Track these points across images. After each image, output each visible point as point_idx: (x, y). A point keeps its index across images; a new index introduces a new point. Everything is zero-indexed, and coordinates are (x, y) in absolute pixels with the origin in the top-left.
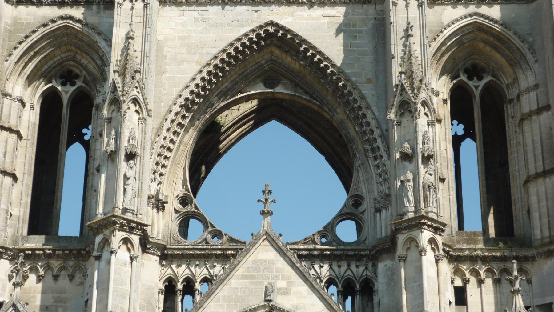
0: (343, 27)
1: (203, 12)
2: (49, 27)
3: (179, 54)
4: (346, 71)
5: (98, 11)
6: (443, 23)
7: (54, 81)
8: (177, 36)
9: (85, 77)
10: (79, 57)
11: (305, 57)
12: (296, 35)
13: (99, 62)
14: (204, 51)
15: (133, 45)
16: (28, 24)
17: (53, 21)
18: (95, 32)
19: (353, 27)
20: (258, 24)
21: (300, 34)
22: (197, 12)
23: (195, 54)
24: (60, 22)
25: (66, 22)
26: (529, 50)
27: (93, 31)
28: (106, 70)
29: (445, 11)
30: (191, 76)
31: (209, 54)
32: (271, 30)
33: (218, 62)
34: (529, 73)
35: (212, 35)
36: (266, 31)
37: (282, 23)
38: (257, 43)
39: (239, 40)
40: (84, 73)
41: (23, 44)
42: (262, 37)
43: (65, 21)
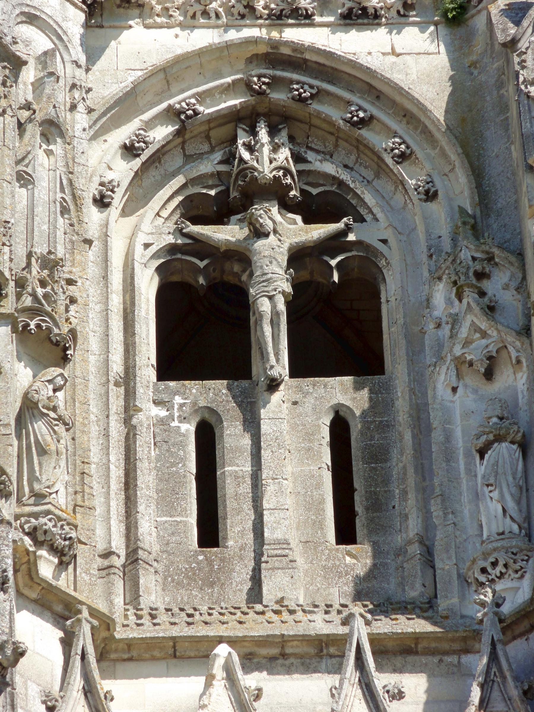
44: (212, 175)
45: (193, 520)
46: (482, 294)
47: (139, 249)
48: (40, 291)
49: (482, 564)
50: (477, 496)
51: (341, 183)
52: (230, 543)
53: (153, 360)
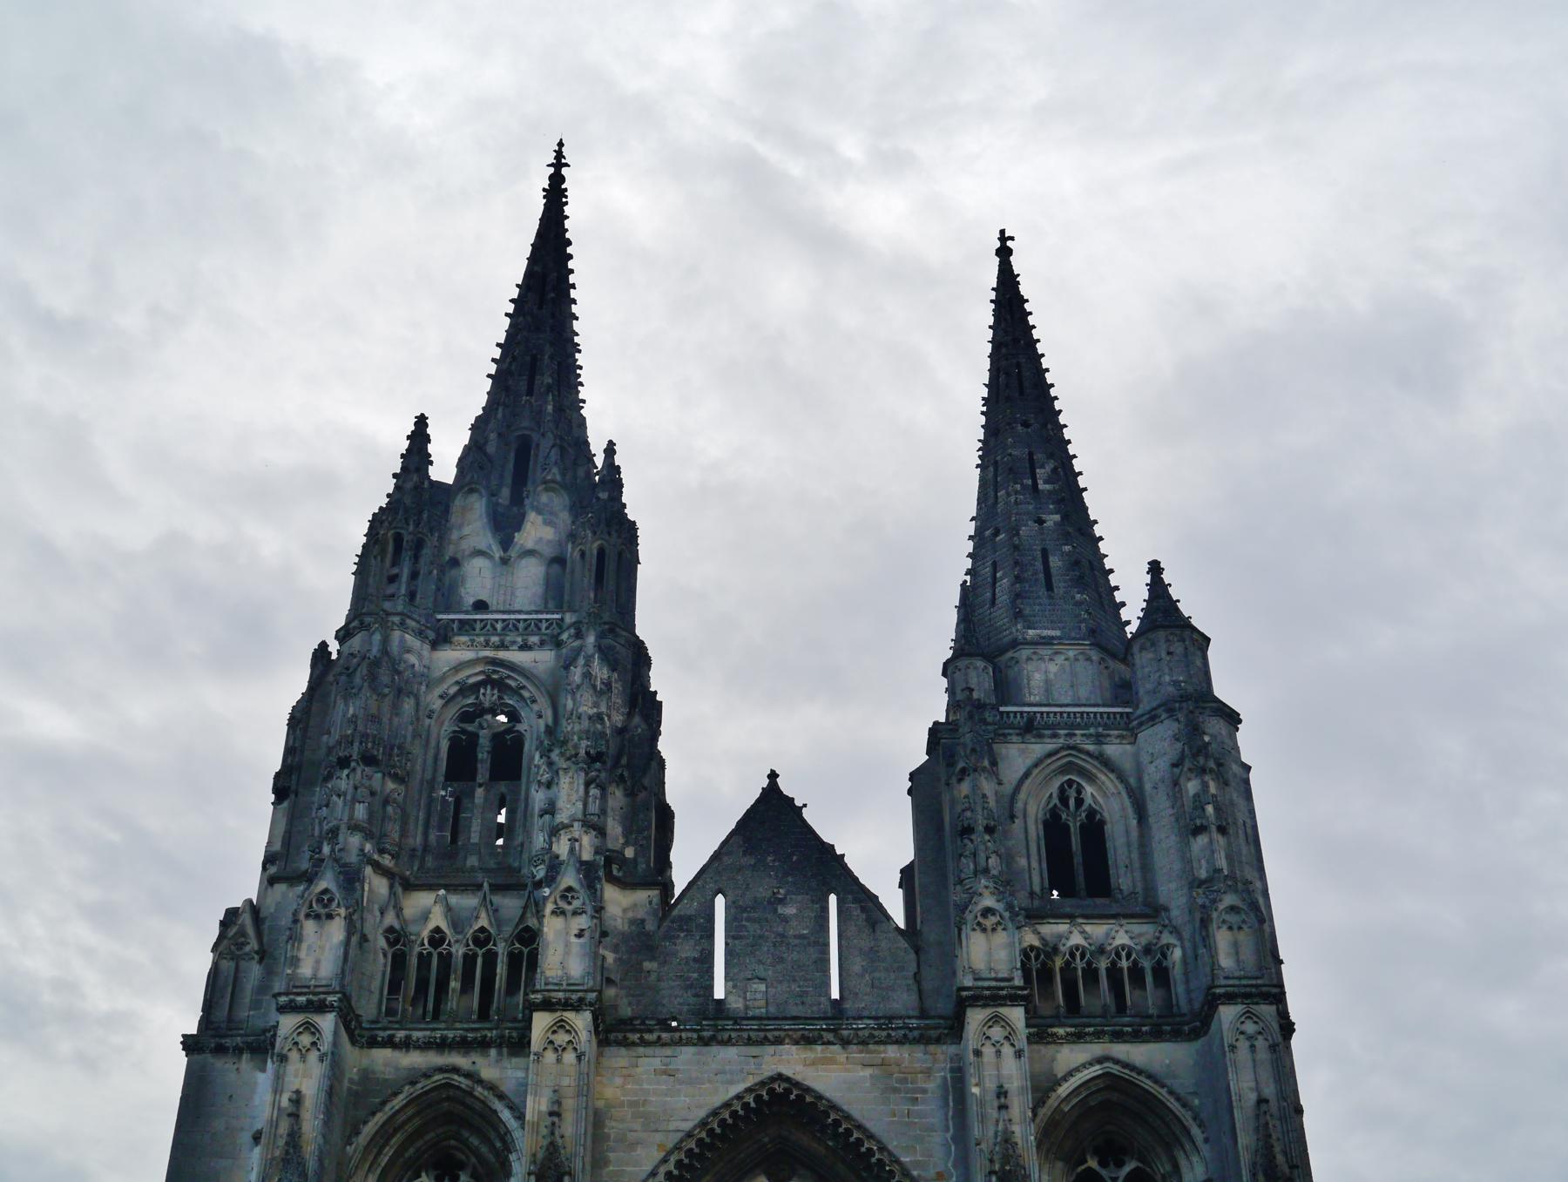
0: (896, 1083)
1: (669, 1059)
2: (419, 1086)
3: (630, 1131)
4: (902, 1159)
5: (500, 1058)
6: (1056, 1076)
7: (423, 1174)
8: (628, 1100)
9: (474, 1168)
10: (466, 1134)
11: (836, 1136)
12: (820, 1097)
13: (498, 1145)
14: (672, 1126)
15: (560, 1127)
16: (386, 1080)
17: (426, 1076)
18: (494, 1095)
19: (911, 1084)
20: (758, 1079)
21: (827, 1095)
22: (659, 1059)
23: (657, 1131)
24: (439, 1077)
25: (447, 1078)
26: (1195, 1119)
27: (491, 1092)
28: (511, 1159)
29: (1059, 1056)
30: (648, 1168)
31: (679, 1131)
32: (779, 1088)
33: (692, 1144)
34: (1195, 1159)
35: (683, 1098)
36: (771, 1092)
37: (798, 1078)
38: (757, 1111)
39: (727, 1105)
40: (473, 1160)
41: (379, 1115)
42: (764, 1101)
43: (446, 1075)
44: (471, 704)
45: (448, 834)
46: (549, 758)
47: (442, 732)
48: (396, 759)
49: (535, 859)
50: (537, 833)
51: (515, 708)
52: (460, 843)
53: (444, 773)
